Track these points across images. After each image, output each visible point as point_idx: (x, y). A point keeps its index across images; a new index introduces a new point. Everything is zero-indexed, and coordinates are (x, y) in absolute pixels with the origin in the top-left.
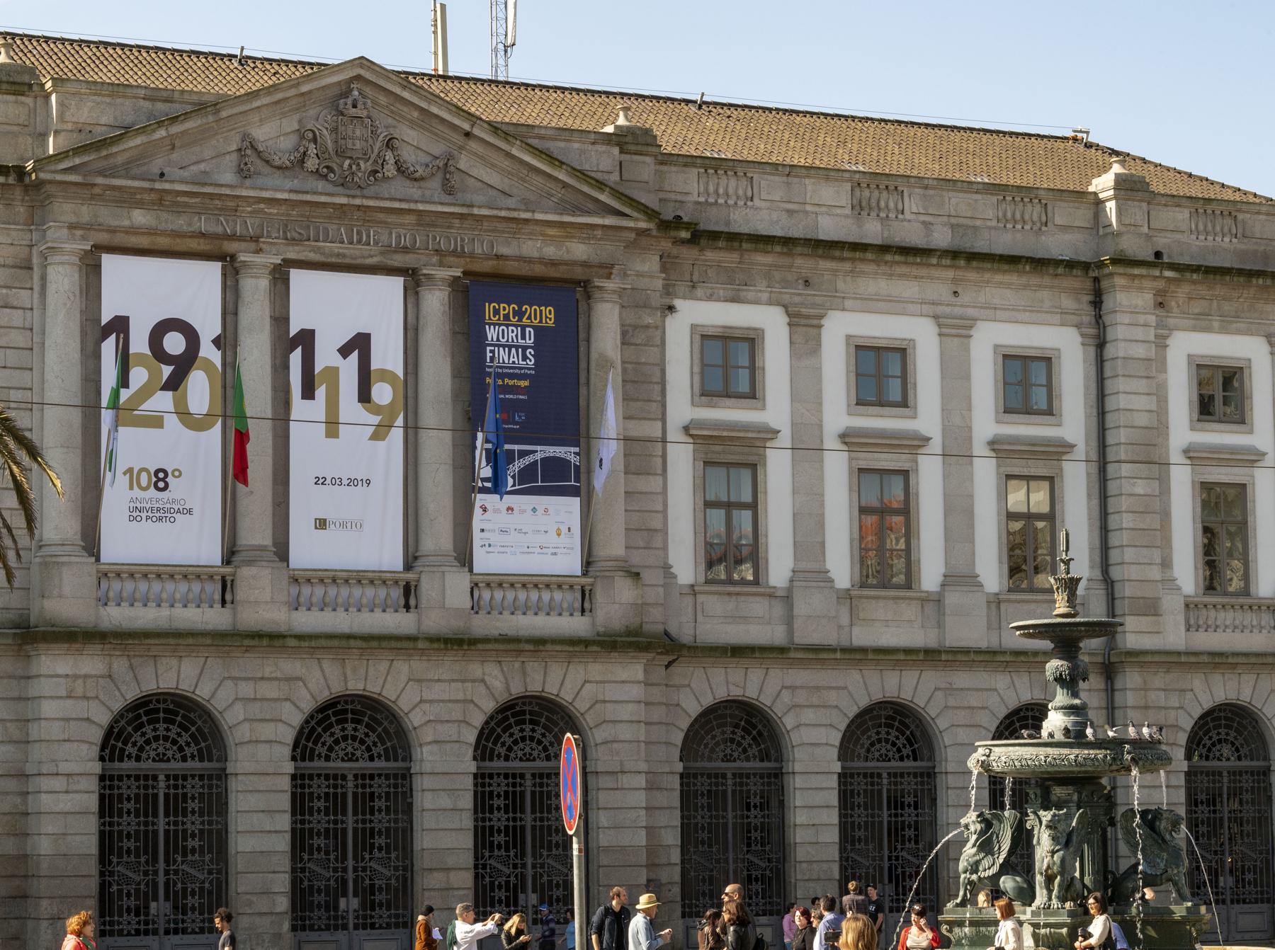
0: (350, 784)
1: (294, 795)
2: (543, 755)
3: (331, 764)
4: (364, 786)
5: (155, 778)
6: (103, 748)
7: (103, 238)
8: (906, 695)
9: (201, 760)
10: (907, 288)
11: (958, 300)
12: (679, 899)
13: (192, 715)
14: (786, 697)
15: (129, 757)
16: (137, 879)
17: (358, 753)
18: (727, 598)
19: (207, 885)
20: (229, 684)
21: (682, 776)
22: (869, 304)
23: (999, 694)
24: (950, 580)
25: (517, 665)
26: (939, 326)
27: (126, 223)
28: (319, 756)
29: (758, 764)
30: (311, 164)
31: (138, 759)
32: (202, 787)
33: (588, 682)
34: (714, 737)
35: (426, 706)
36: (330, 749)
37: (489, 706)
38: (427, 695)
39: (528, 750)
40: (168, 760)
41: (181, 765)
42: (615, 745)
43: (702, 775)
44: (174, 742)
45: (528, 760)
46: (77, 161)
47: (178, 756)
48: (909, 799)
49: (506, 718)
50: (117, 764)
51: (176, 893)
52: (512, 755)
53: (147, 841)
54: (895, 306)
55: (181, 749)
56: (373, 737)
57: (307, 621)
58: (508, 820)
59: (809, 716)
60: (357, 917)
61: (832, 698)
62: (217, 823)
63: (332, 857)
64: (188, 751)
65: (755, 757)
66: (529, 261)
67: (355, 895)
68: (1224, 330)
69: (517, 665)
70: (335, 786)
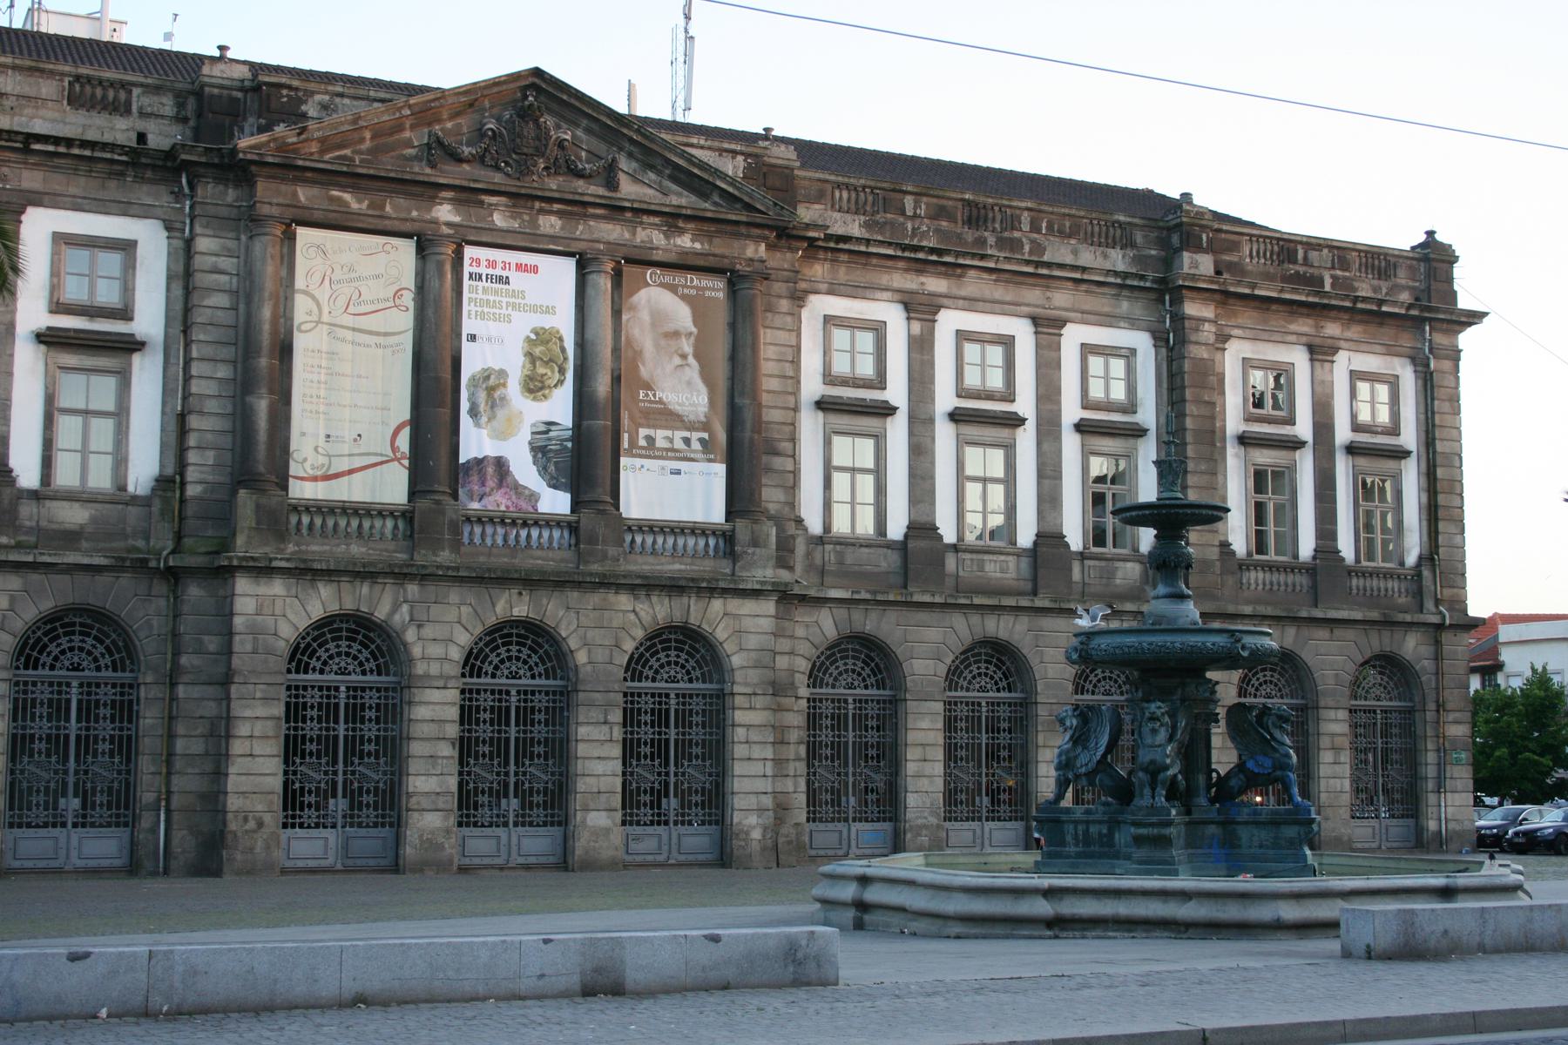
0: (514, 699)
1: (462, 707)
2: (686, 678)
3: (496, 681)
4: (525, 701)
5: (337, 689)
6: (291, 660)
9: (379, 674)
12: (804, 806)
13: (372, 635)
15: (314, 670)
16: (318, 778)
17: (521, 672)
19: (381, 785)
21: (809, 700)
28: (486, 673)
29: (875, 692)
31: (322, 672)
32: (379, 698)
34: (837, 668)
36: (496, 668)
37: (640, 634)
39: (672, 673)
40: (349, 674)
41: (361, 678)
43: (827, 700)
44: (355, 658)
45: (673, 682)
47: (358, 670)
49: (654, 645)
50: (302, 676)
51: (352, 792)
52: (659, 677)
53: (329, 745)
55: (361, 664)
56: (535, 658)
58: (653, 733)
60: (517, 816)
62: (392, 730)
63: (495, 762)
64: (367, 667)
67: (515, 797)
70: (500, 701)
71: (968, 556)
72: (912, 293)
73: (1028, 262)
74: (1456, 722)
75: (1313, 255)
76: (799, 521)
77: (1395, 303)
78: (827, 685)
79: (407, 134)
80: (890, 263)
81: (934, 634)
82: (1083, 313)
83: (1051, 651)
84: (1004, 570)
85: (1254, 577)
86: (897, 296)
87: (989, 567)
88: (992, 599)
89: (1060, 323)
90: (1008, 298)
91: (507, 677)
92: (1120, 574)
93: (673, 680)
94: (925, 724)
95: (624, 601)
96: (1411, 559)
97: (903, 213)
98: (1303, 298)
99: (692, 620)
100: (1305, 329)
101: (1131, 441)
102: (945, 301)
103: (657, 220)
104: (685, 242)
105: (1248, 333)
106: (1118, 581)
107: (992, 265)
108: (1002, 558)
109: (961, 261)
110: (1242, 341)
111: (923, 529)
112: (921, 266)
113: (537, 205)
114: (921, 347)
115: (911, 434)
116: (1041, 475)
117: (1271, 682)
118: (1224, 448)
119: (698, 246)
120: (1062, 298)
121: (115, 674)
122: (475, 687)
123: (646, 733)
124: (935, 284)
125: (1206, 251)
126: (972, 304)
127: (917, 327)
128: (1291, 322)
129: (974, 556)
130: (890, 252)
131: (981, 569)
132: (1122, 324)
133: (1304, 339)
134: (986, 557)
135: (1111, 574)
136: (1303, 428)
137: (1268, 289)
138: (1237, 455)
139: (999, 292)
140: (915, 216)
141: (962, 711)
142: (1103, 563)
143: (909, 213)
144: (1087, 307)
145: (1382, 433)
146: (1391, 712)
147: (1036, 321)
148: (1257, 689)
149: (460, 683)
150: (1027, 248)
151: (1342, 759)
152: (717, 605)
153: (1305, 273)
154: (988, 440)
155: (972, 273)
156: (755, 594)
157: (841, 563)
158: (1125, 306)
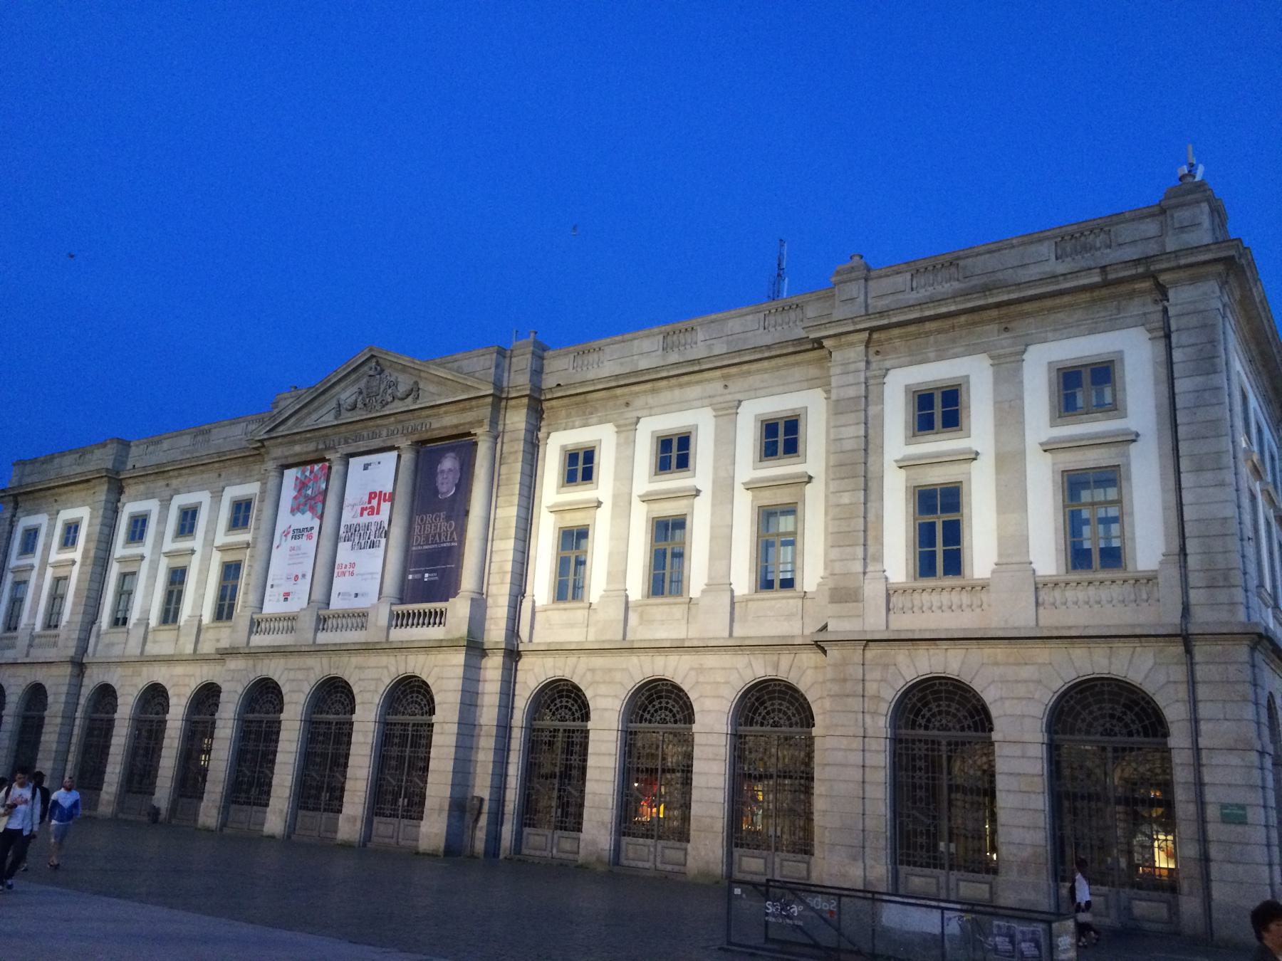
7: (284, 462)
10: (694, 392)
11: (727, 391)
14: (589, 676)
18: (563, 612)
20: (286, 672)
22: (666, 409)
23: (738, 672)
24: (711, 587)
25: (404, 657)
26: (715, 410)
27: (292, 452)
30: (360, 405)
33: (436, 666)
35: (360, 683)
38: (362, 676)
42: (445, 706)
46: (268, 429)
54: (684, 405)
57: (323, 638)
59: (603, 689)
61: (618, 676)
65: (578, 719)
66: (445, 428)
68: (940, 358)
69: (404, 657)
78: (757, 723)
91: (1102, 734)
93: (946, 728)
121: (974, 734)
122: (571, 728)
123: (395, 751)
141: (920, 750)
148: (652, 716)
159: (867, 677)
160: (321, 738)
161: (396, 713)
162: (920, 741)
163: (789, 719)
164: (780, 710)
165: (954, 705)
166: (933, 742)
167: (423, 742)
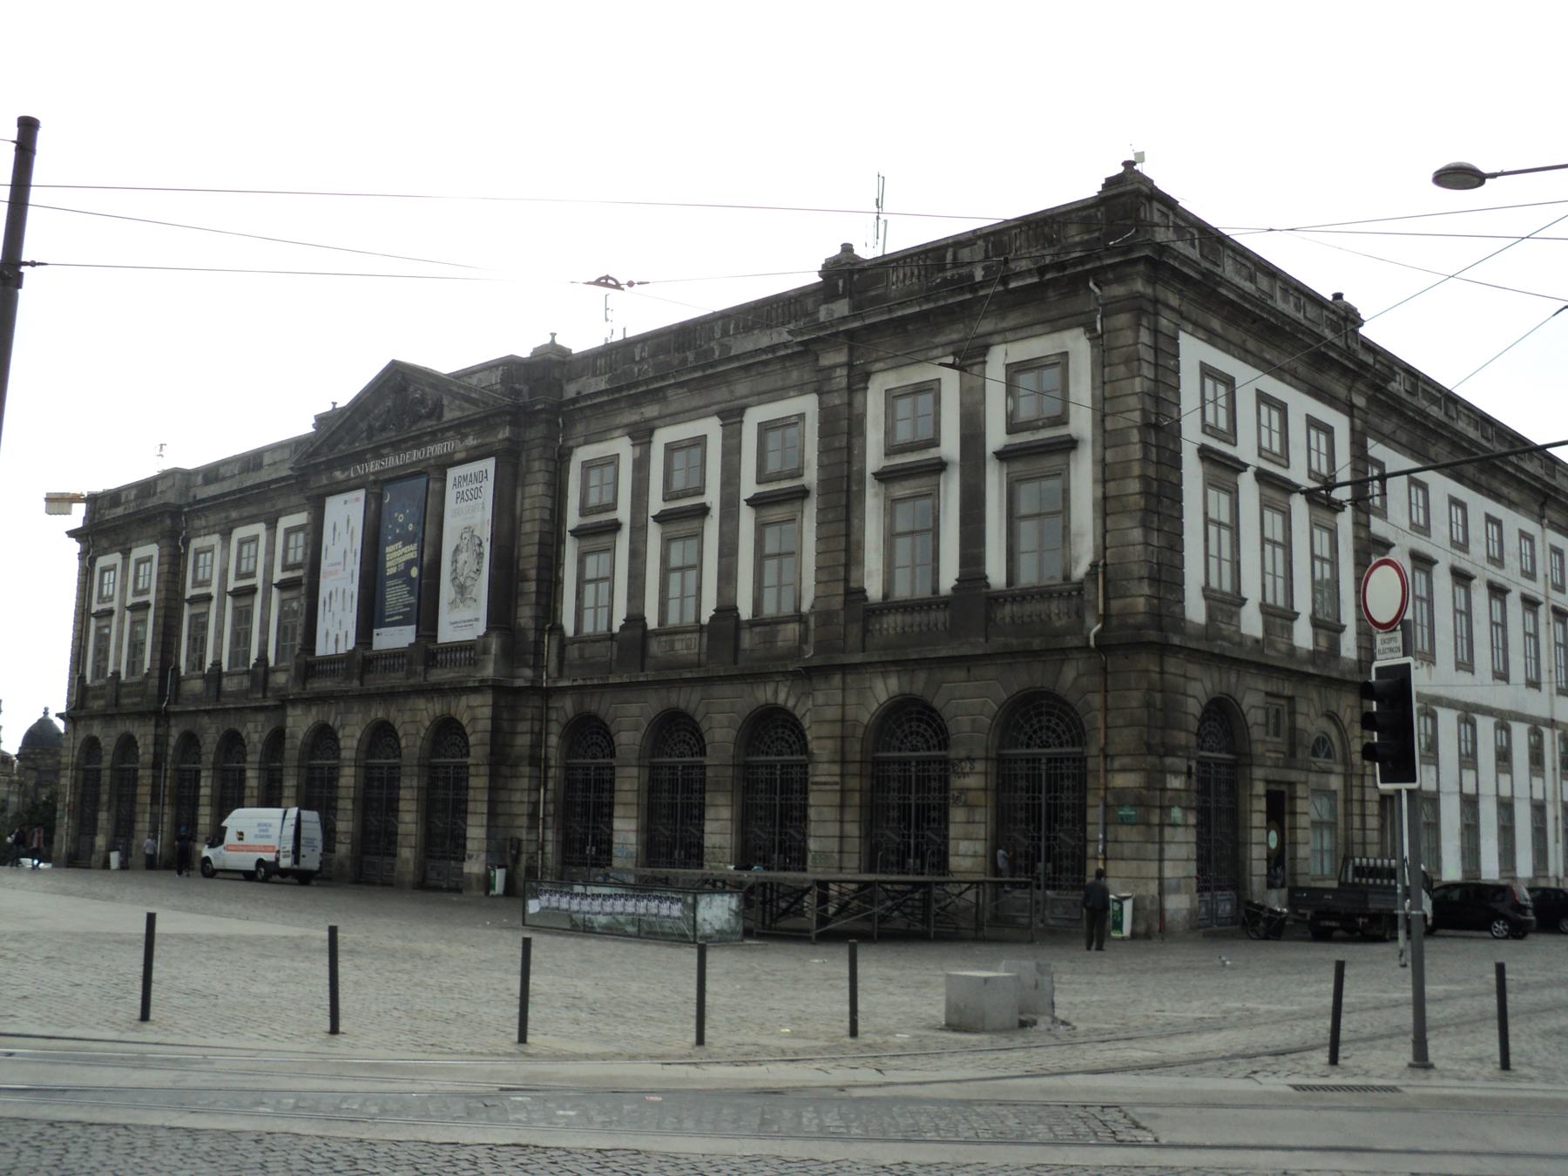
8: (682, 705)
26: (722, 419)
37: (427, 723)
48: (796, 786)
71: (664, 638)
72: (636, 423)
73: (695, 369)
74: (1123, 770)
75: (965, 254)
76: (560, 629)
77: (1020, 275)
79: (361, 425)
80: (615, 407)
81: (634, 708)
82: (758, 394)
83: (718, 716)
84: (685, 648)
85: (892, 622)
86: (626, 430)
87: (678, 646)
88: (672, 676)
89: (741, 411)
90: (701, 404)
92: (781, 637)
94: (626, 786)
95: (421, 703)
96: (1080, 571)
97: (633, 360)
98: (917, 309)
99: (452, 713)
100: (955, 336)
101: (798, 503)
102: (657, 423)
103: (451, 433)
104: (471, 441)
105: (890, 363)
106: (780, 644)
107: (672, 381)
108: (688, 636)
109: (651, 387)
110: (885, 374)
111: (635, 619)
112: (636, 401)
113: (403, 446)
114: (641, 466)
115: (631, 542)
116: (721, 555)
117: (917, 733)
118: (862, 492)
119: (475, 442)
120: (742, 388)
124: (651, 411)
125: (842, 296)
126: (675, 418)
127: (638, 449)
128: (935, 336)
129: (669, 638)
130: (605, 398)
131: (672, 648)
132: (792, 394)
133: (950, 349)
134: (677, 637)
135: (770, 639)
136: (950, 447)
137: (876, 315)
138: (877, 495)
139: (697, 401)
140: (642, 359)
142: (768, 628)
143: (637, 358)
144: (763, 388)
145: (1044, 427)
146: (792, 766)
147: (722, 415)
149: (952, 754)
150: (717, 353)
151: (977, 818)
152: (464, 701)
153: (953, 276)
154: (683, 533)
155: (670, 393)
156: (476, 690)
157: (581, 656)
158: (795, 375)
159: (848, 702)
160: (376, 784)
161: (373, 757)
162: (1068, 760)
163: (1059, 737)
164: (1048, 728)
165: (1054, 720)
166: (1034, 761)
167: (607, 786)
